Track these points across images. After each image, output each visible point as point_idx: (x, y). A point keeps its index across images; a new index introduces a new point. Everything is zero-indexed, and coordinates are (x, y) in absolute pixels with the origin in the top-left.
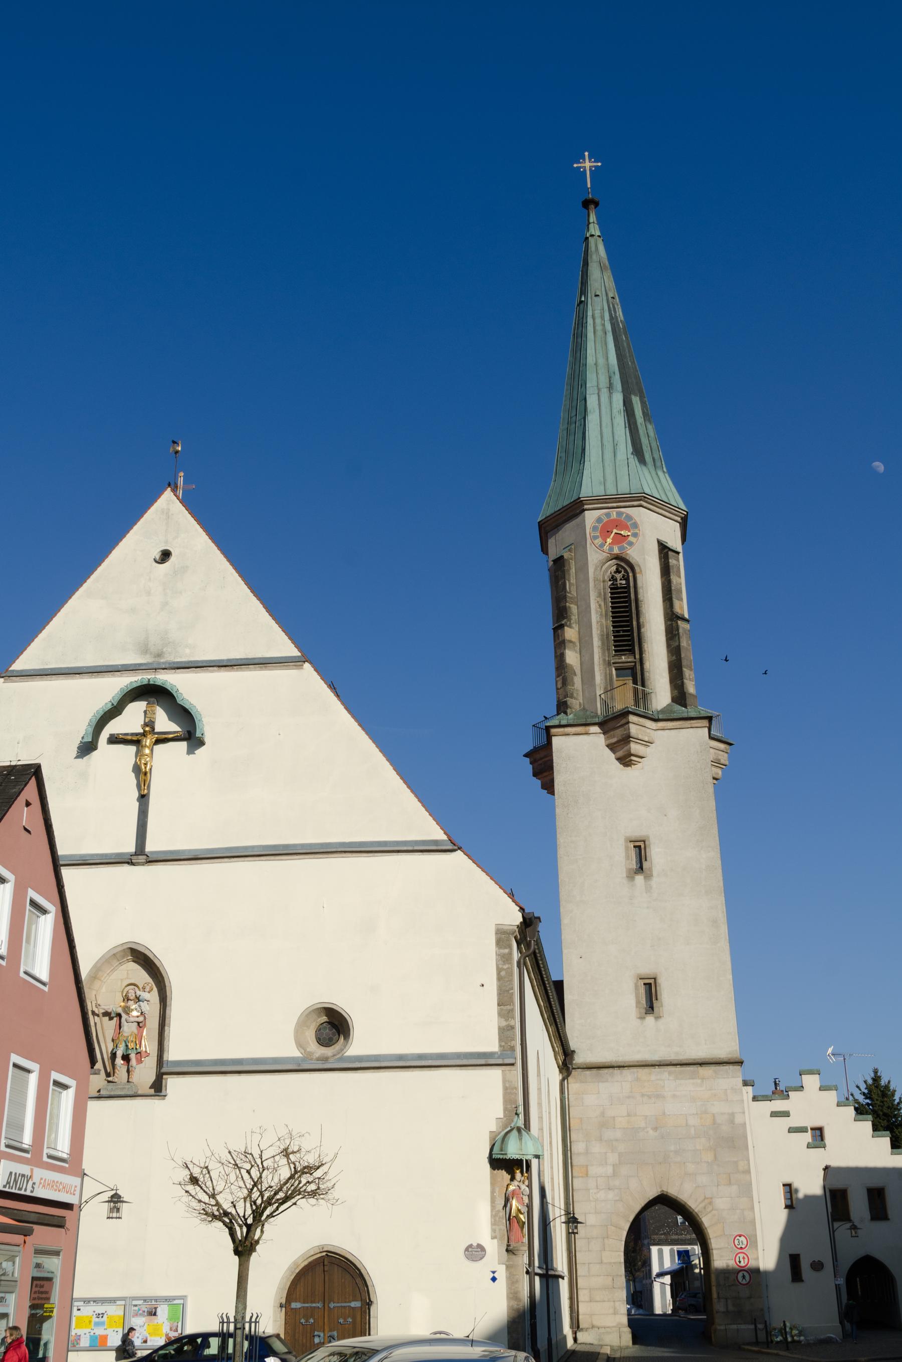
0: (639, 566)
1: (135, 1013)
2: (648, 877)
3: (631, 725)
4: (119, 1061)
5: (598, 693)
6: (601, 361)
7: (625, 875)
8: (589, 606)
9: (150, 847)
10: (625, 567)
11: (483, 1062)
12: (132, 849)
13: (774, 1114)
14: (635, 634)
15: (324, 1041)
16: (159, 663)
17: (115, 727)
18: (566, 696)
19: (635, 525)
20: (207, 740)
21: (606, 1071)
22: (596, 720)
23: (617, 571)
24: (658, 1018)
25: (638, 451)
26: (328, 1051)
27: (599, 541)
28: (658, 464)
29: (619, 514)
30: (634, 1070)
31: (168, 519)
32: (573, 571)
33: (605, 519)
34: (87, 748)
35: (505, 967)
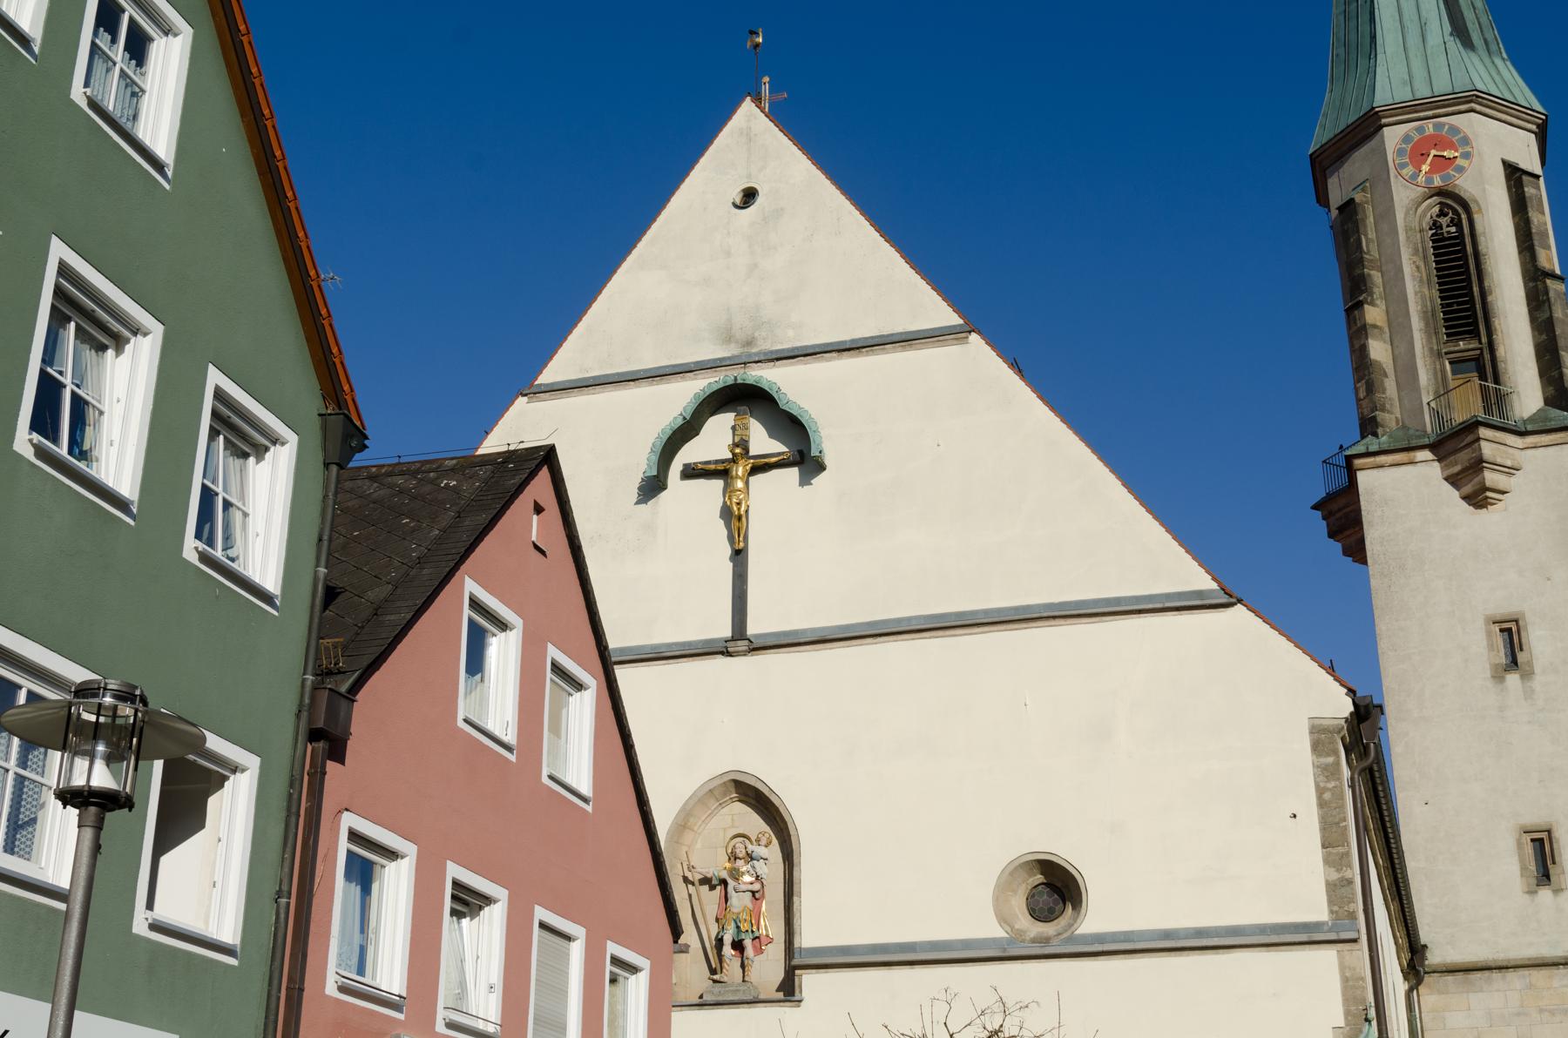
0: (1476, 202)
1: (747, 878)
2: (1527, 675)
3: (1483, 444)
4: (728, 950)
5: (1425, 401)
7: (1488, 674)
8: (1400, 270)
9: (752, 629)
11: (1304, 938)
12: (727, 632)
14: (1478, 306)
15: (1041, 913)
16: (750, 355)
17: (692, 453)
18: (1375, 409)
19: (1466, 141)
20: (828, 460)
21: (1478, 975)
22: (1426, 441)
23: (1442, 214)
24: (1557, 891)
25: (1460, 31)
27: (1408, 171)
28: (1493, 47)
29: (1438, 126)
30: (1525, 972)
31: (751, 143)
32: (1371, 220)
33: (1416, 137)
34: (652, 487)
35: (1331, 785)
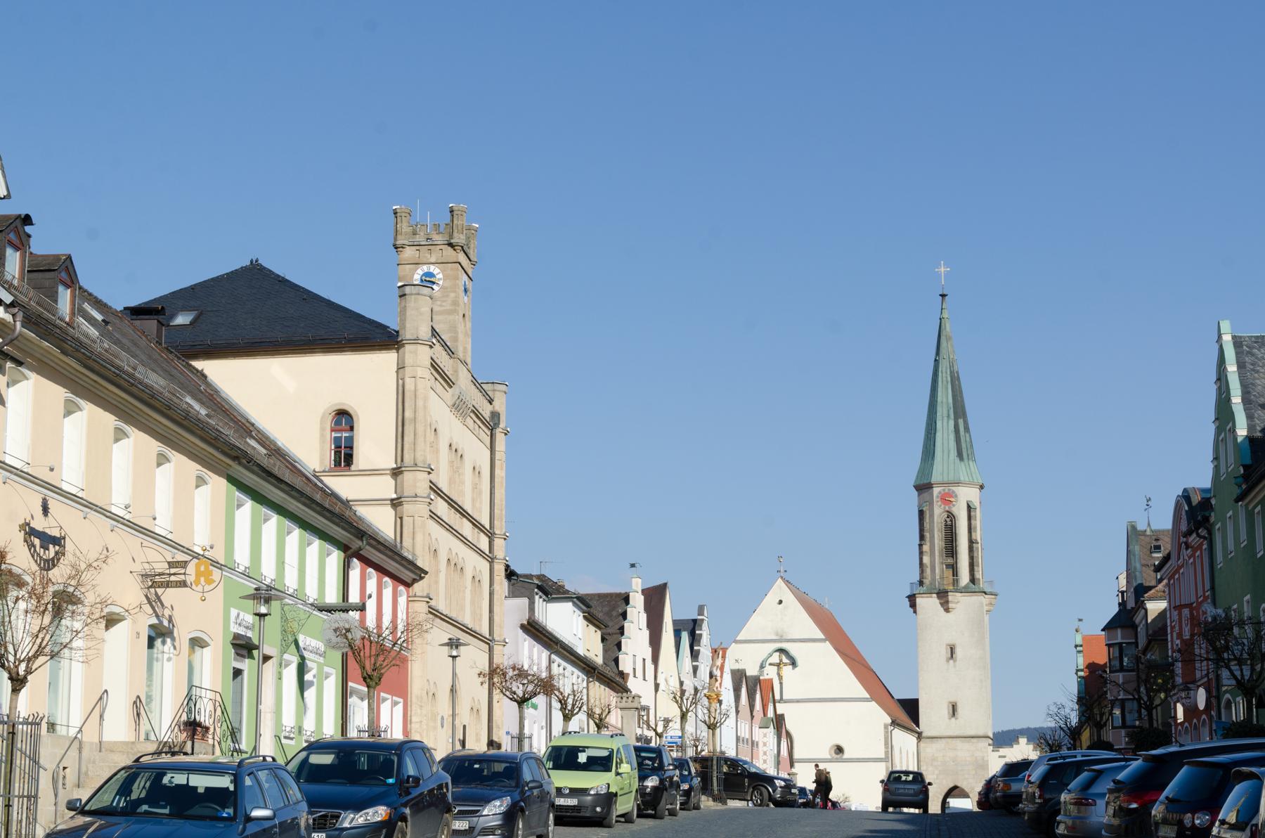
10: (951, 516)
17: (770, 660)
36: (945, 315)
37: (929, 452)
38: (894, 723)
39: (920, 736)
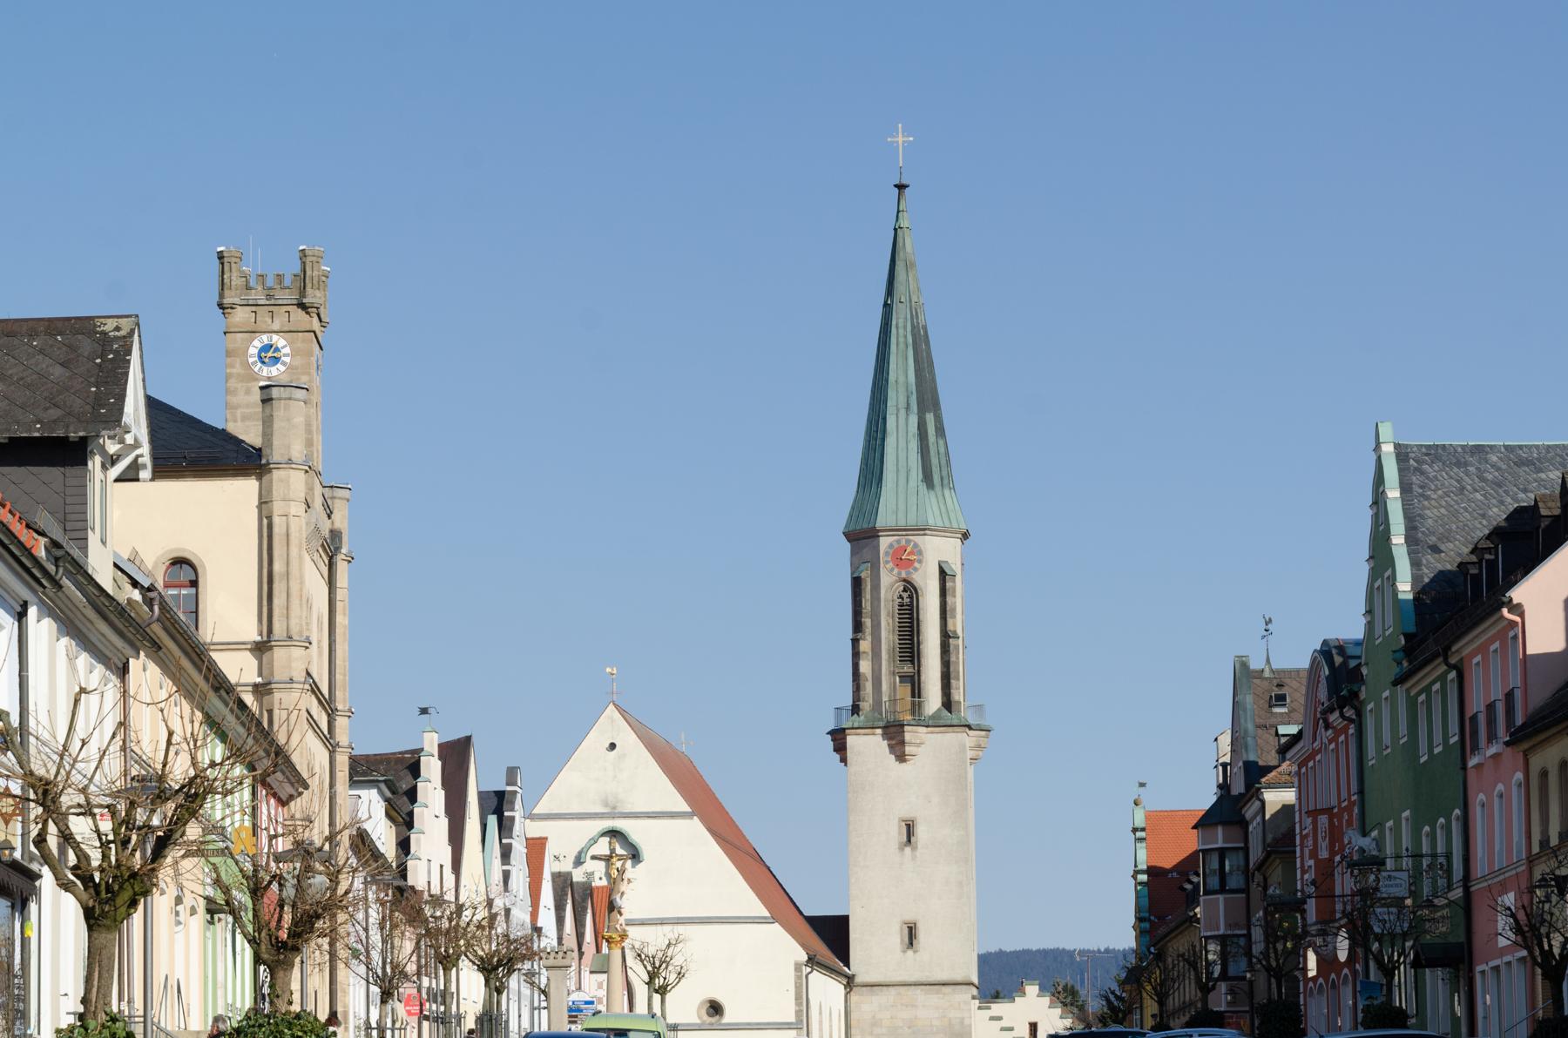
2: (914, 849)
6: (902, 379)
10: (911, 590)
13: (992, 1018)
15: (710, 1015)
19: (920, 553)
25: (928, 478)
26: (713, 1020)
36: (904, 223)
37: (871, 473)
38: (812, 961)
39: (850, 982)
